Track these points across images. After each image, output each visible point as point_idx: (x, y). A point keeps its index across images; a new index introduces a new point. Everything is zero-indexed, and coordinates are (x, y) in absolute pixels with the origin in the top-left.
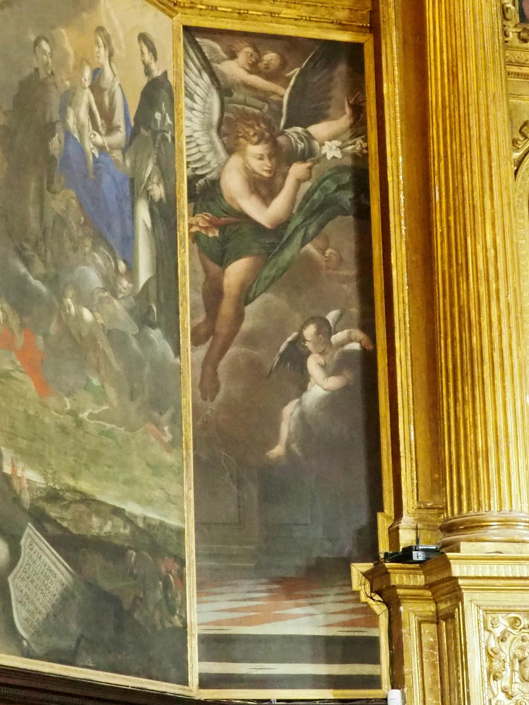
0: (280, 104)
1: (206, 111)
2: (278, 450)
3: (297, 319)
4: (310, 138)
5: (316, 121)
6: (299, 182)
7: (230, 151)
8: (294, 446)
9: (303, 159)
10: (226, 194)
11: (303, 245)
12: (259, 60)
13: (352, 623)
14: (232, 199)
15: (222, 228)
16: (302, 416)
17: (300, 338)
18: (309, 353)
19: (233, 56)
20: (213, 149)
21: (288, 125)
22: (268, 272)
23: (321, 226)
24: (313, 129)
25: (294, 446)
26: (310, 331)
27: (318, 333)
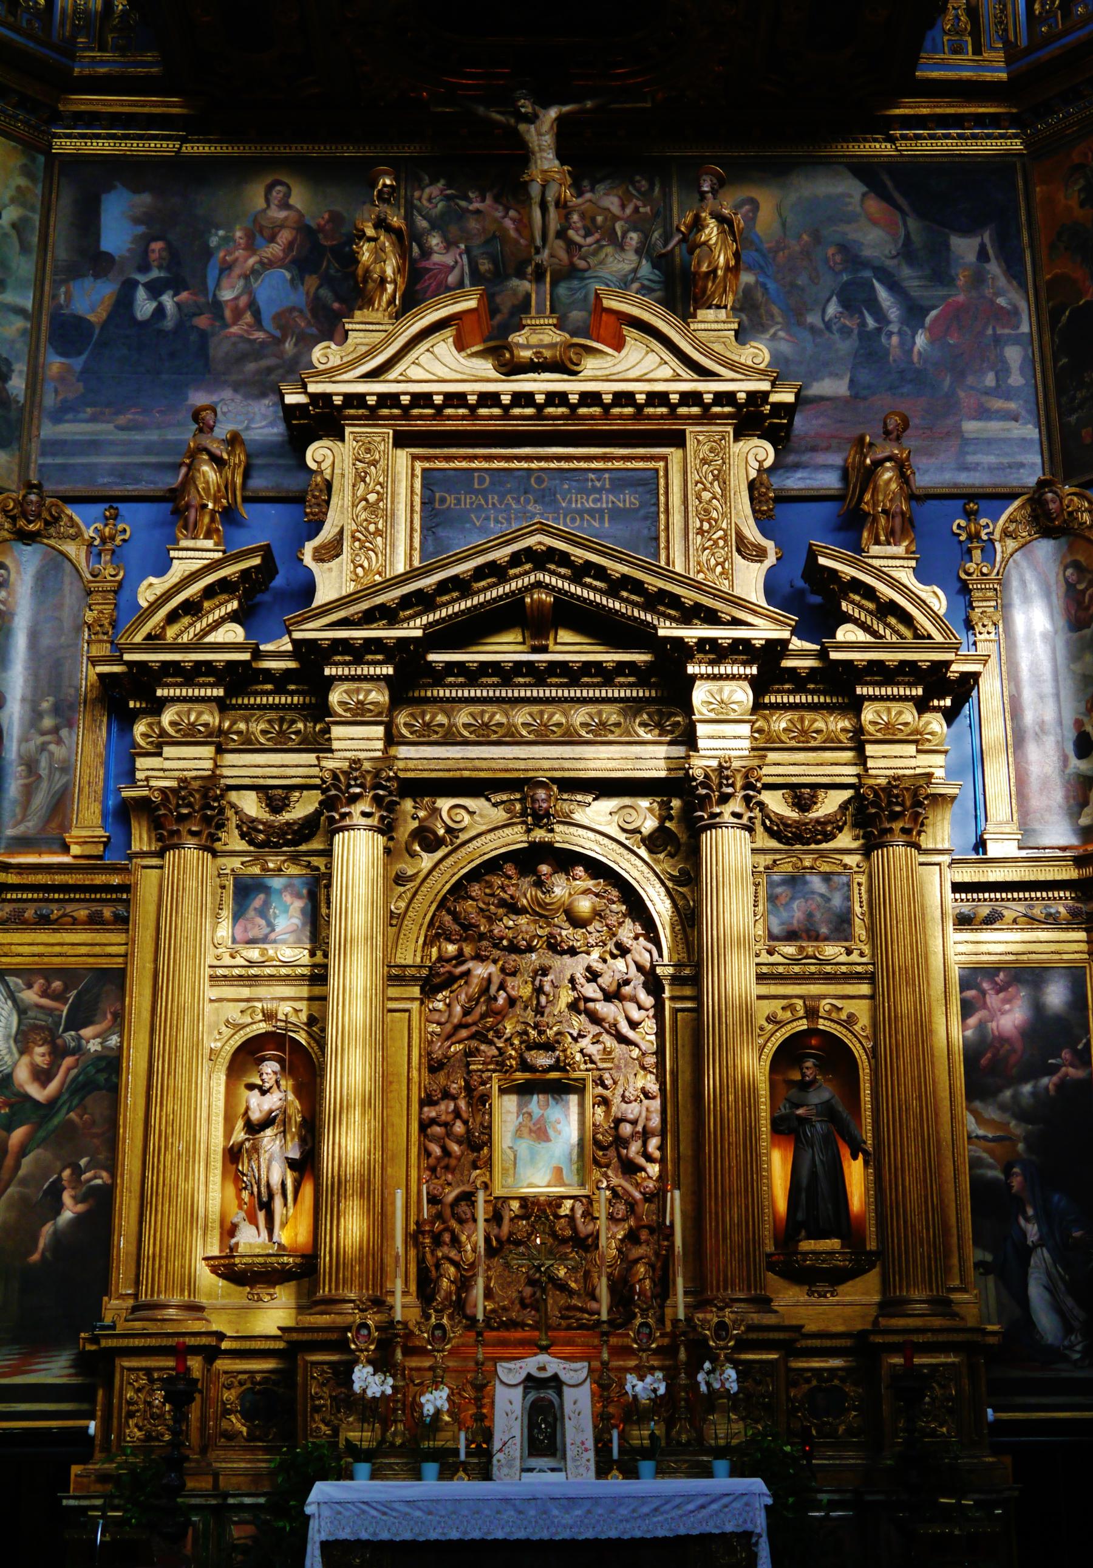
0: (60, 1016)
1: (8, 1027)
2: (36, 1257)
3: (59, 1164)
4: (80, 1038)
5: (85, 1025)
6: (69, 1069)
7: (22, 1053)
8: (48, 1254)
9: (72, 1052)
10: (16, 1082)
11: (68, 1113)
12: (49, 986)
13: (69, 1375)
14: (21, 1086)
15: (11, 1106)
16: (55, 1232)
17: (60, 1179)
18: (64, 1189)
19: (30, 986)
20: (10, 1052)
21: (65, 1031)
22: (41, 1134)
23: (82, 1099)
24: (83, 1032)
25: (48, 1254)
26: (66, 1173)
27: (73, 1173)
